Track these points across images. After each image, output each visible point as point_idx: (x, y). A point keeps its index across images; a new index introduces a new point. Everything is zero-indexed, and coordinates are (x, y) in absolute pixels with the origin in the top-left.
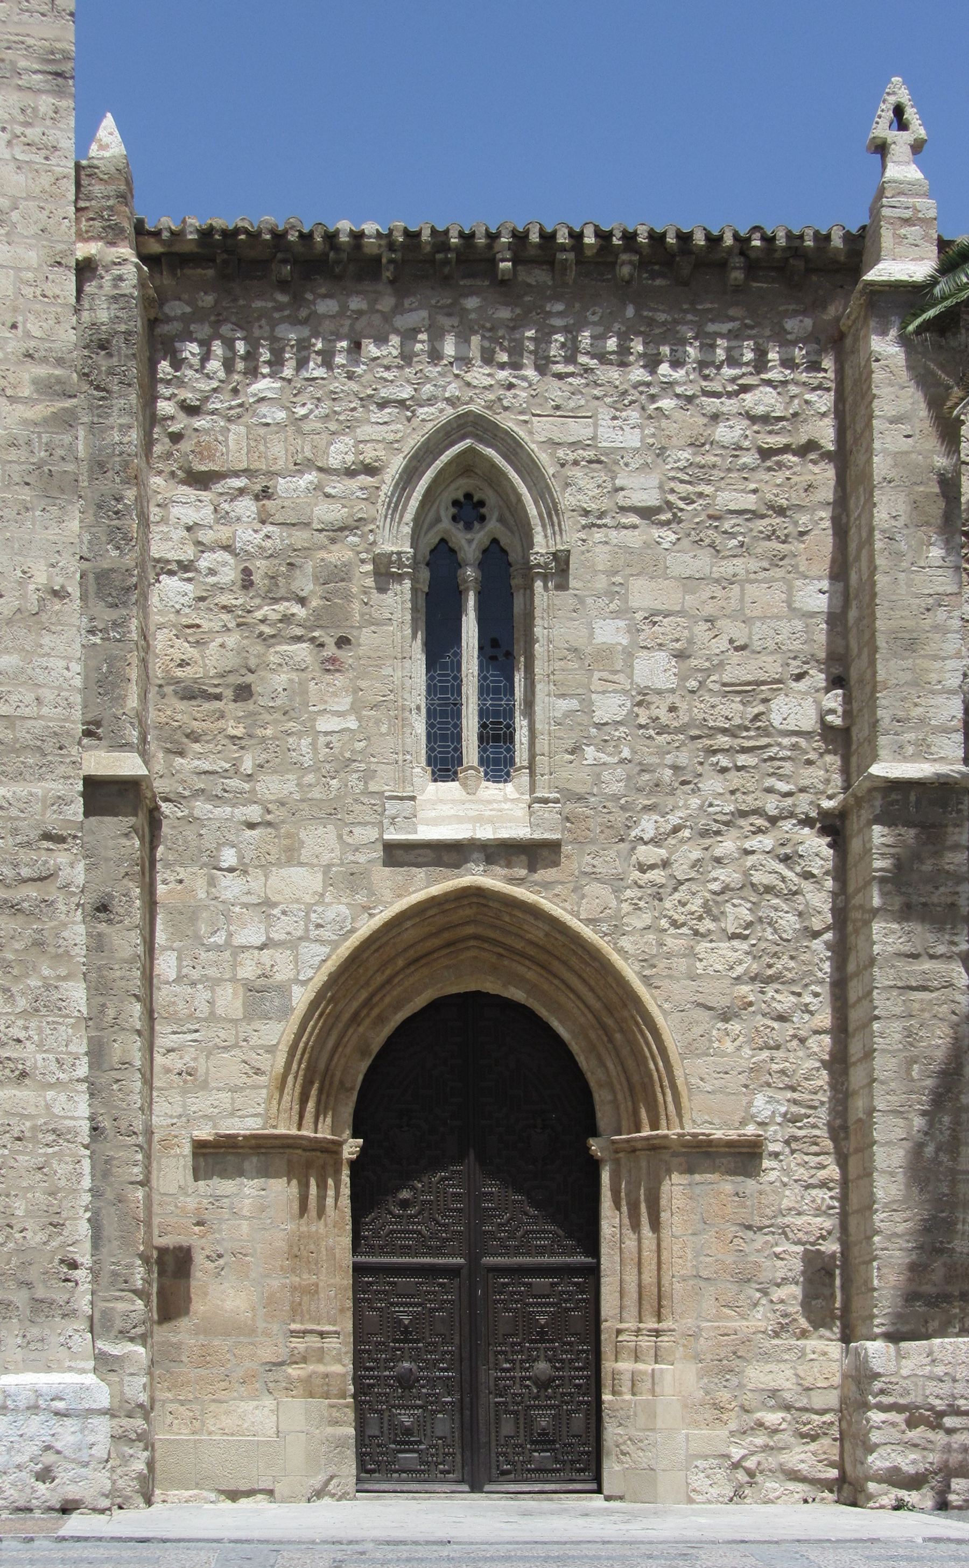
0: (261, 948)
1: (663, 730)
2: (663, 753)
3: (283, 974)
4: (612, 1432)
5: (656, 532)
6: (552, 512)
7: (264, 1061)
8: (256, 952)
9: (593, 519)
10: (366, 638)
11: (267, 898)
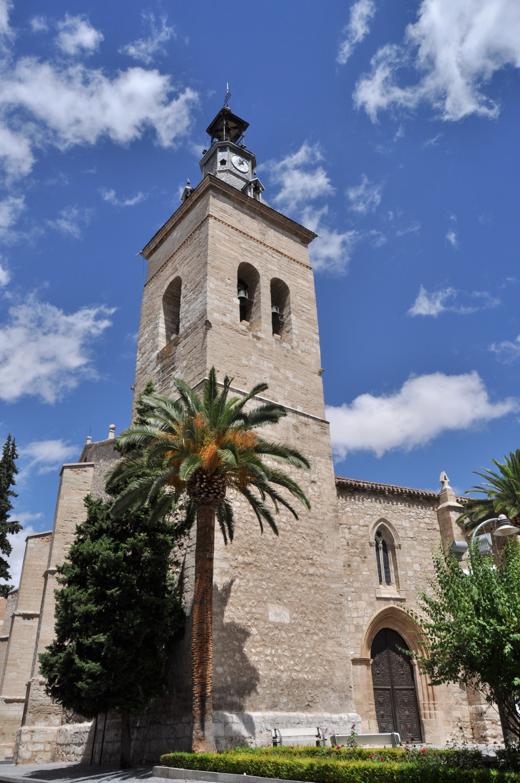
1: (419, 578)
2: (420, 582)
3: (361, 623)
4: (426, 728)
5: (414, 542)
6: (398, 536)
7: (359, 642)
9: (404, 539)
10: (369, 557)
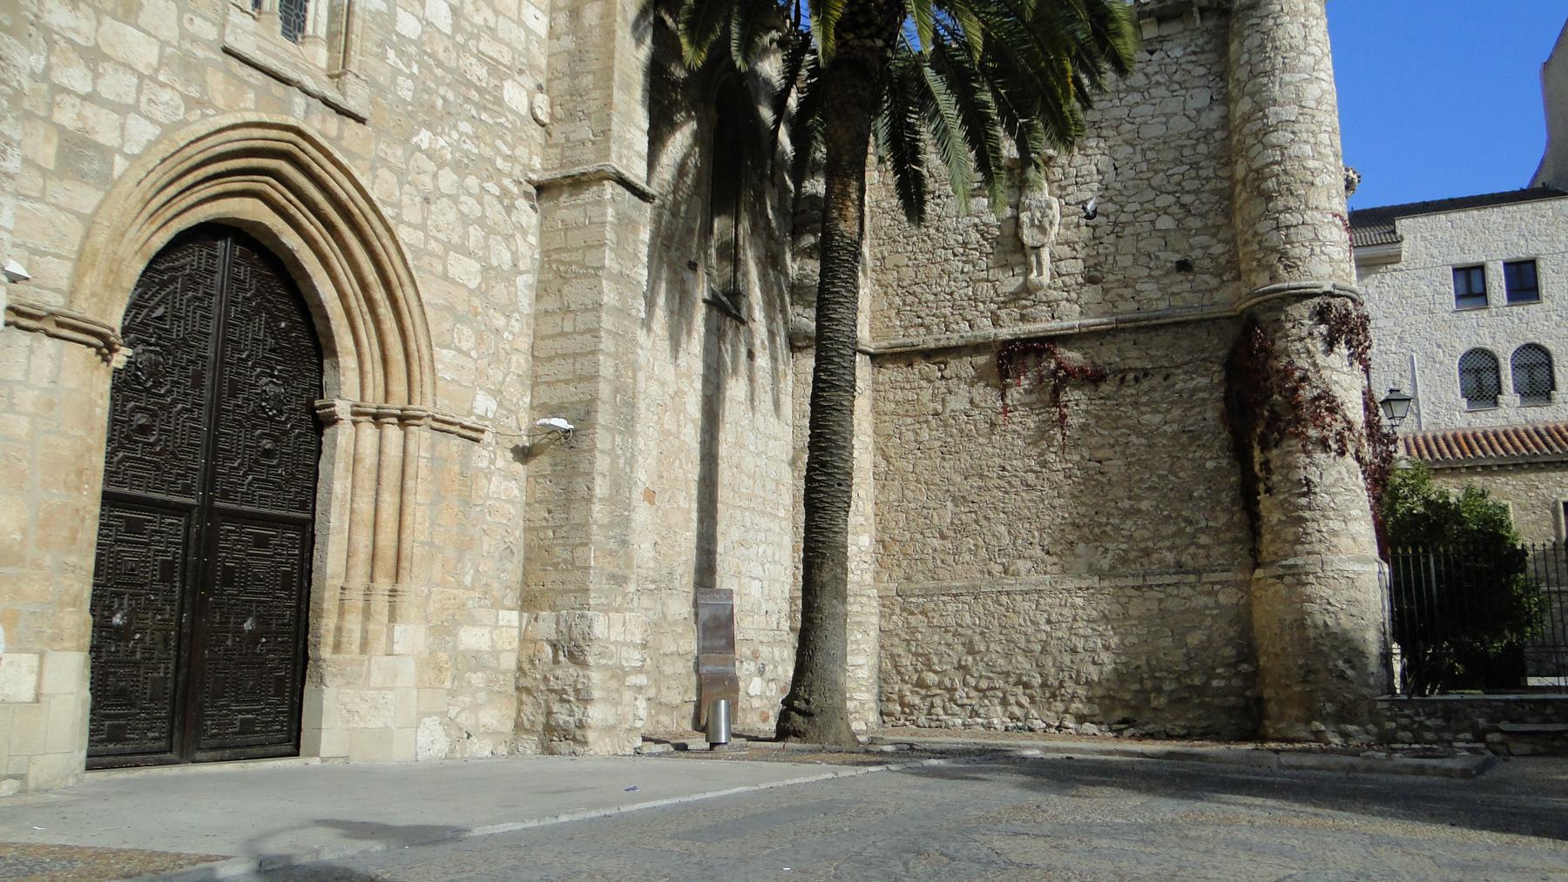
0: (85, 98)
1: (440, 64)
3: (106, 136)
8: (77, 101)
11: (97, 46)
